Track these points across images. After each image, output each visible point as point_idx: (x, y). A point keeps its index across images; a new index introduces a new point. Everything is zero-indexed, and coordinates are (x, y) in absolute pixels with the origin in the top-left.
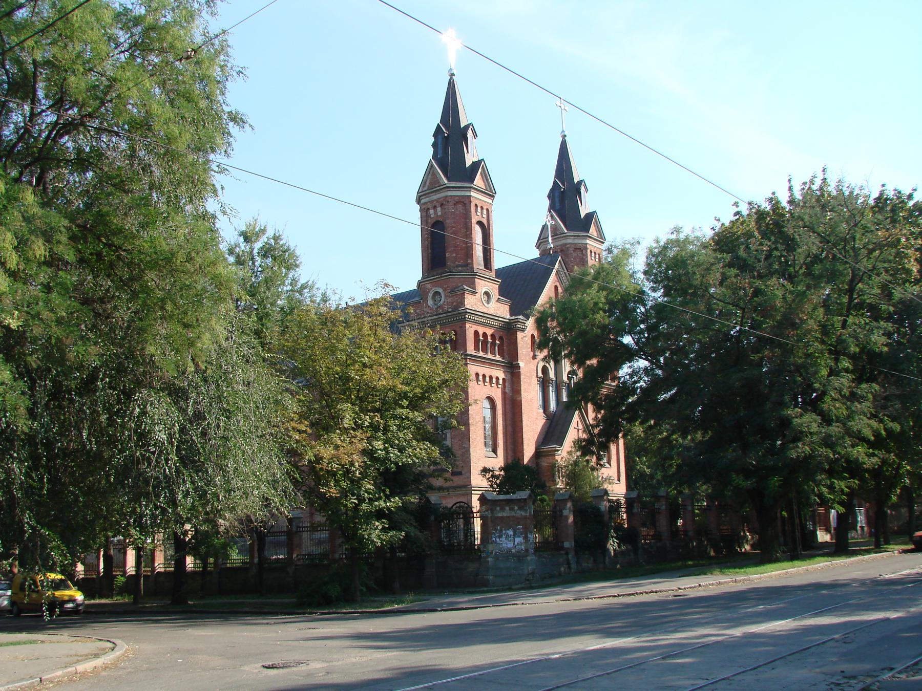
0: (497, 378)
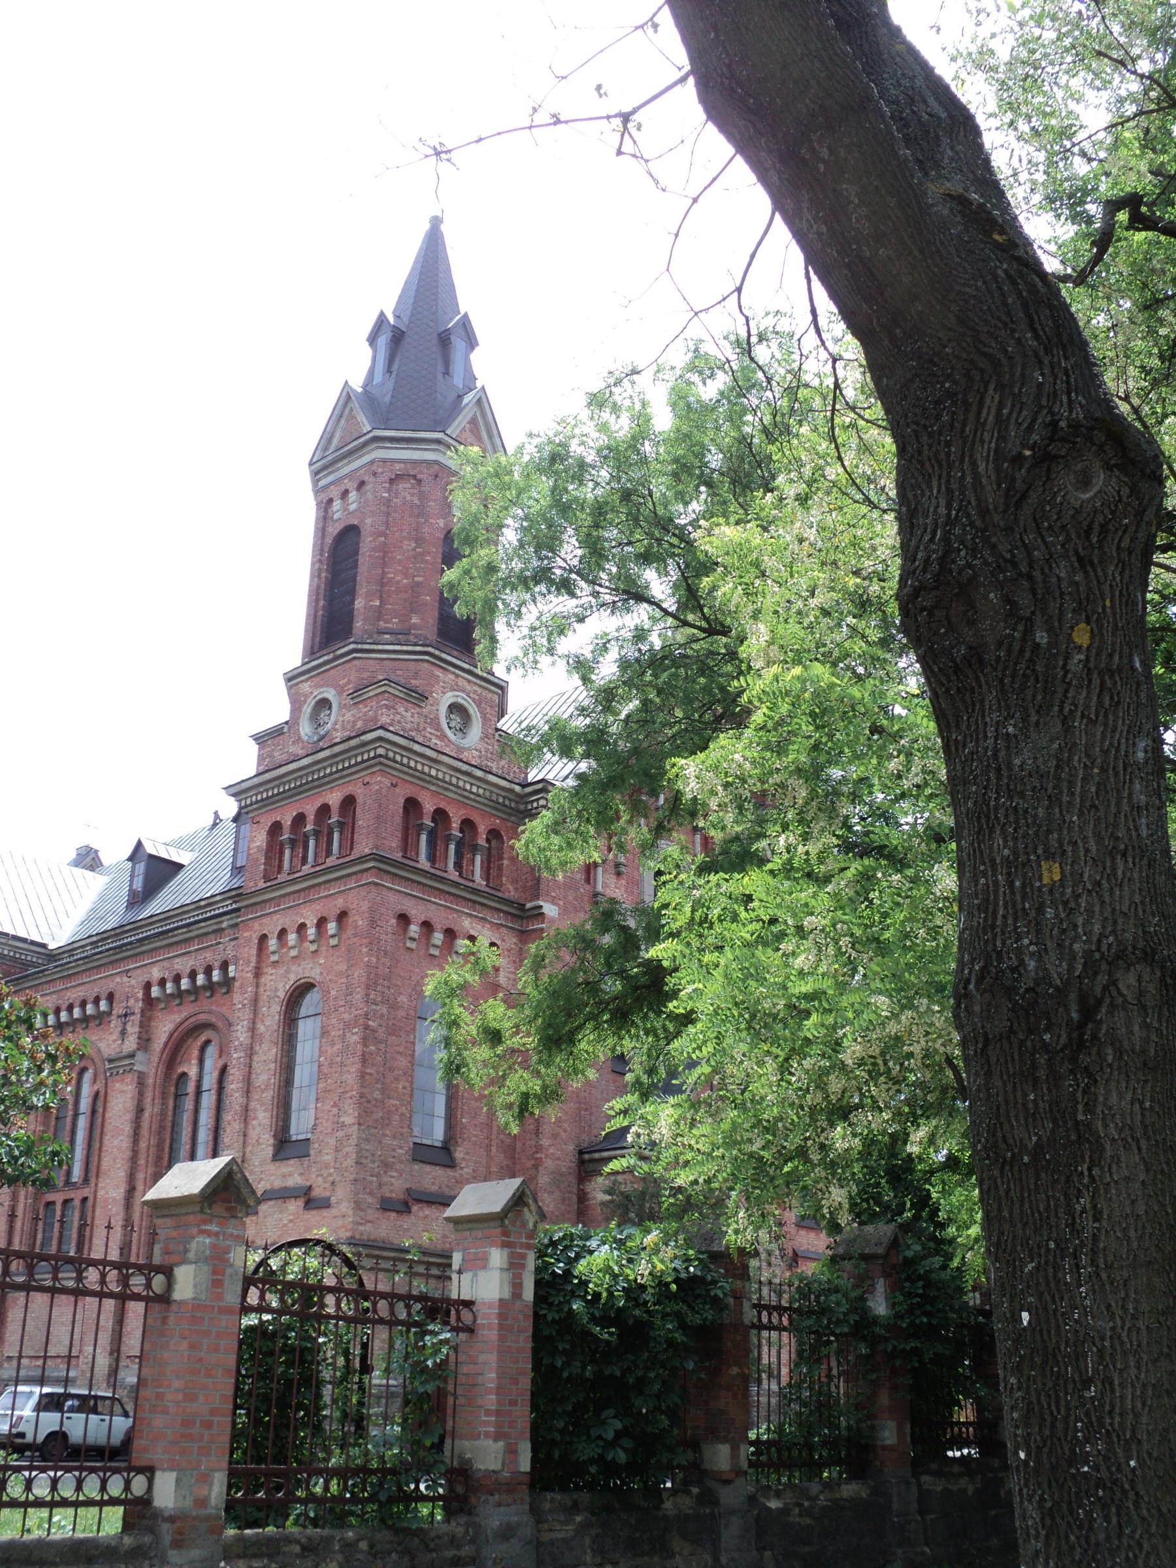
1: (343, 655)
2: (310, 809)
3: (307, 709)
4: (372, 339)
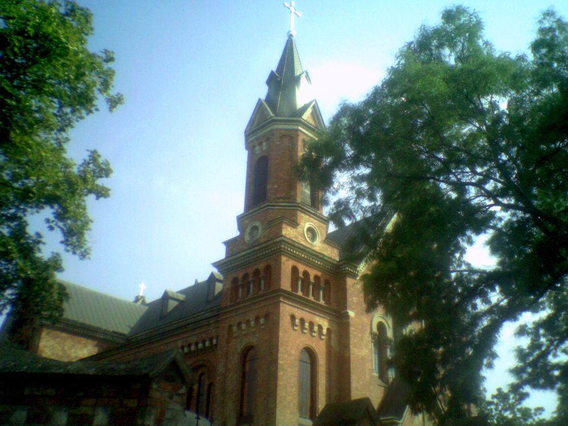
0: (320, 327)
1: (263, 208)
2: (251, 271)
3: (248, 230)
4: (269, 82)
